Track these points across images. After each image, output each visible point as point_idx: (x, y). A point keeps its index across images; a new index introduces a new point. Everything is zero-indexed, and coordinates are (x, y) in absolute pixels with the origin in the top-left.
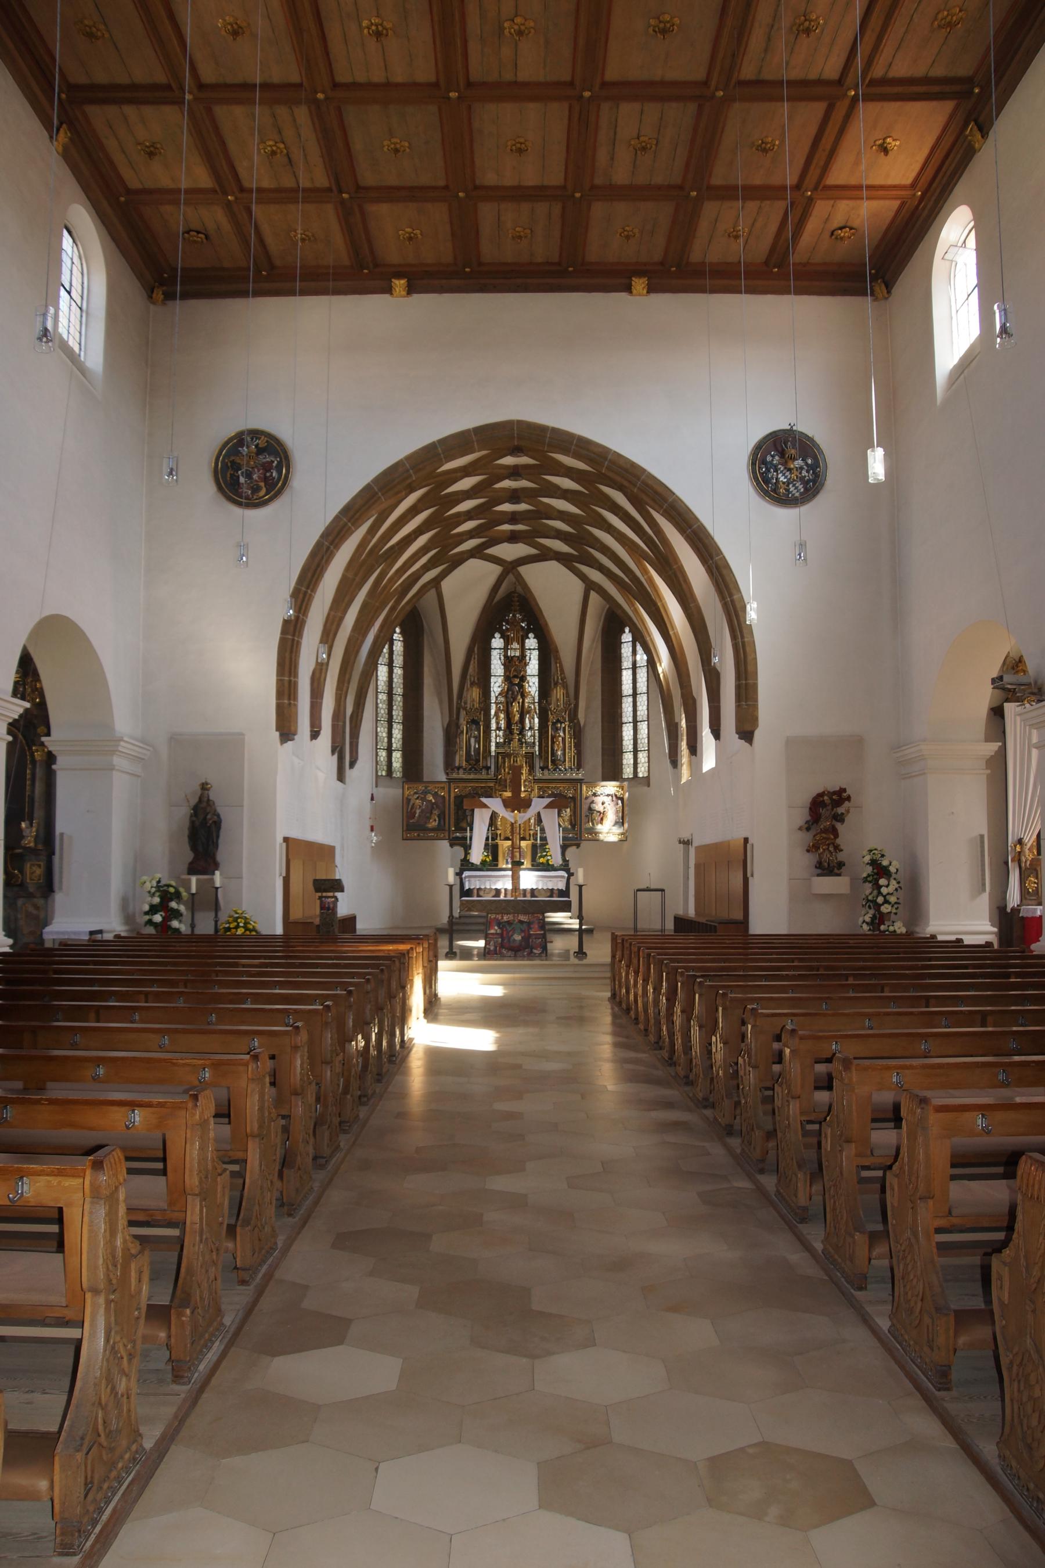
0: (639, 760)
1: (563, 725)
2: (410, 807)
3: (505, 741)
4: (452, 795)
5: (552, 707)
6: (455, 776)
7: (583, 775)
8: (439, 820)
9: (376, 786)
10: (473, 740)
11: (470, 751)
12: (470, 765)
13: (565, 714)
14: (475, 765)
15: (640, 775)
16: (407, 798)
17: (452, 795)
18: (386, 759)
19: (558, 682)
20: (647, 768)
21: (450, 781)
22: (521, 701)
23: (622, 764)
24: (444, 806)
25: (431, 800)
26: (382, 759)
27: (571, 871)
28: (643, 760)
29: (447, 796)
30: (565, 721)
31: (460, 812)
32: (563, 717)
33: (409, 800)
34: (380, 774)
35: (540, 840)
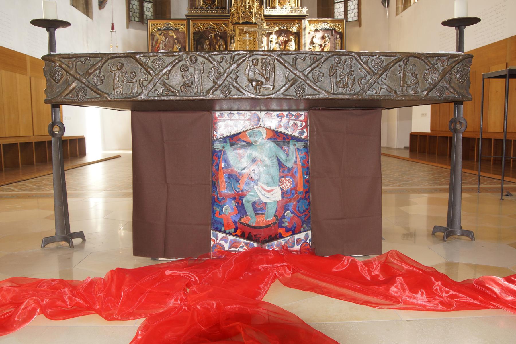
0: (349, 8)
2: (154, 42)
4: (192, 31)
6: (193, 13)
7: (307, 12)
9: (128, 27)
12: (207, 5)
14: (211, 5)
15: (350, 20)
16: (151, 34)
17: (192, 31)
18: (138, 7)
20: (357, 14)
21: (189, 18)
23: (334, 13)
24: (185, 42)
25: (173, 35)
26: (134, 7)
28: (353, 7)
29: (186, 32)
31: (199, 46)
33: (153, 36)
34: (133, 19)
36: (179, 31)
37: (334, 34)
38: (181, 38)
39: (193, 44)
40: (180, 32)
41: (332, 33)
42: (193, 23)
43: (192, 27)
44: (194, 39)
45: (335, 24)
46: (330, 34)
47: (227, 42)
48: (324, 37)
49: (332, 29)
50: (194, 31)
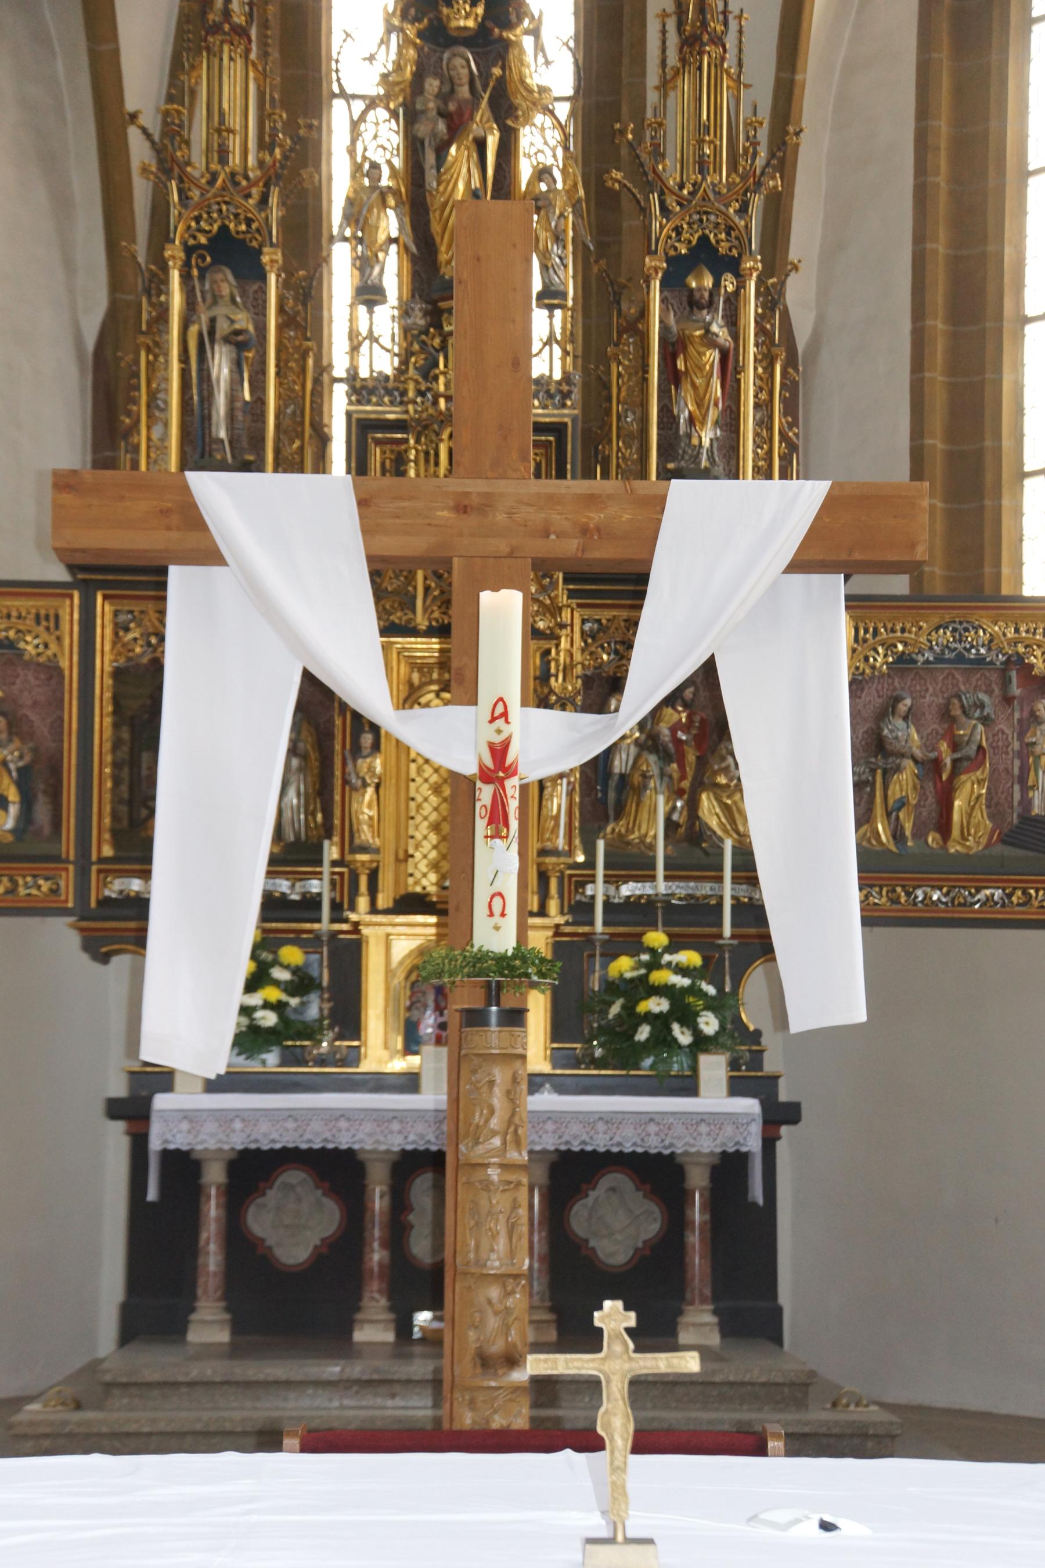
1: (729, 284)
3: (401, 371)
4: (104, 662)
5: (670, 171)
8: (27, 803)
10: (221, 367)
11: (206, 419)
13: (743, 210)
17: (104, 662)
19: (704, 24)
22: (492, 142)
27: (783, 1096)
29: (69, 663)
30: (743, 244)
32: (729, 229)
35: (605, 923)
36: (21, 653)
37: (1016, 690)
38: (35, 704)
39: (108, 746)
40: (27, 665)
41: (1006, 683)
42: (116, 613)
43: (108, 631)
44: (117, 711)
45: (1023, 628)
46: (989, 692)
47: (331, 736)
48: (957, 712)
49: (1007, 662)
50: (122, 661)
